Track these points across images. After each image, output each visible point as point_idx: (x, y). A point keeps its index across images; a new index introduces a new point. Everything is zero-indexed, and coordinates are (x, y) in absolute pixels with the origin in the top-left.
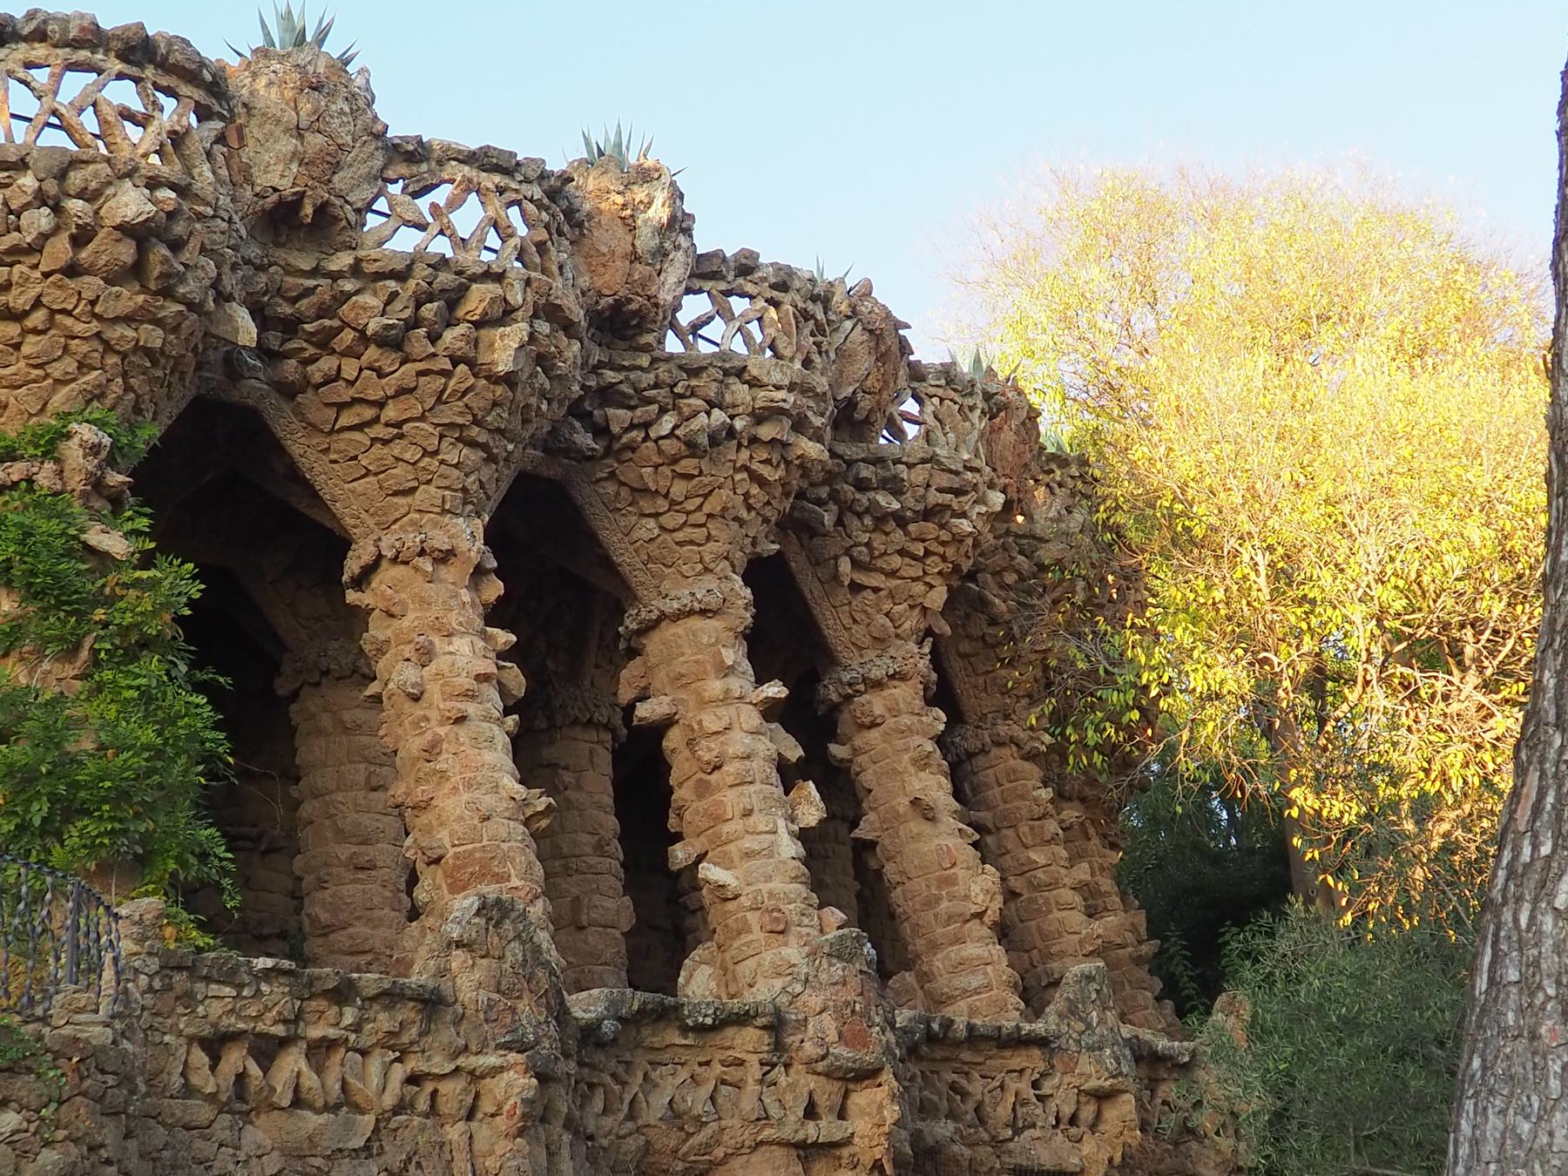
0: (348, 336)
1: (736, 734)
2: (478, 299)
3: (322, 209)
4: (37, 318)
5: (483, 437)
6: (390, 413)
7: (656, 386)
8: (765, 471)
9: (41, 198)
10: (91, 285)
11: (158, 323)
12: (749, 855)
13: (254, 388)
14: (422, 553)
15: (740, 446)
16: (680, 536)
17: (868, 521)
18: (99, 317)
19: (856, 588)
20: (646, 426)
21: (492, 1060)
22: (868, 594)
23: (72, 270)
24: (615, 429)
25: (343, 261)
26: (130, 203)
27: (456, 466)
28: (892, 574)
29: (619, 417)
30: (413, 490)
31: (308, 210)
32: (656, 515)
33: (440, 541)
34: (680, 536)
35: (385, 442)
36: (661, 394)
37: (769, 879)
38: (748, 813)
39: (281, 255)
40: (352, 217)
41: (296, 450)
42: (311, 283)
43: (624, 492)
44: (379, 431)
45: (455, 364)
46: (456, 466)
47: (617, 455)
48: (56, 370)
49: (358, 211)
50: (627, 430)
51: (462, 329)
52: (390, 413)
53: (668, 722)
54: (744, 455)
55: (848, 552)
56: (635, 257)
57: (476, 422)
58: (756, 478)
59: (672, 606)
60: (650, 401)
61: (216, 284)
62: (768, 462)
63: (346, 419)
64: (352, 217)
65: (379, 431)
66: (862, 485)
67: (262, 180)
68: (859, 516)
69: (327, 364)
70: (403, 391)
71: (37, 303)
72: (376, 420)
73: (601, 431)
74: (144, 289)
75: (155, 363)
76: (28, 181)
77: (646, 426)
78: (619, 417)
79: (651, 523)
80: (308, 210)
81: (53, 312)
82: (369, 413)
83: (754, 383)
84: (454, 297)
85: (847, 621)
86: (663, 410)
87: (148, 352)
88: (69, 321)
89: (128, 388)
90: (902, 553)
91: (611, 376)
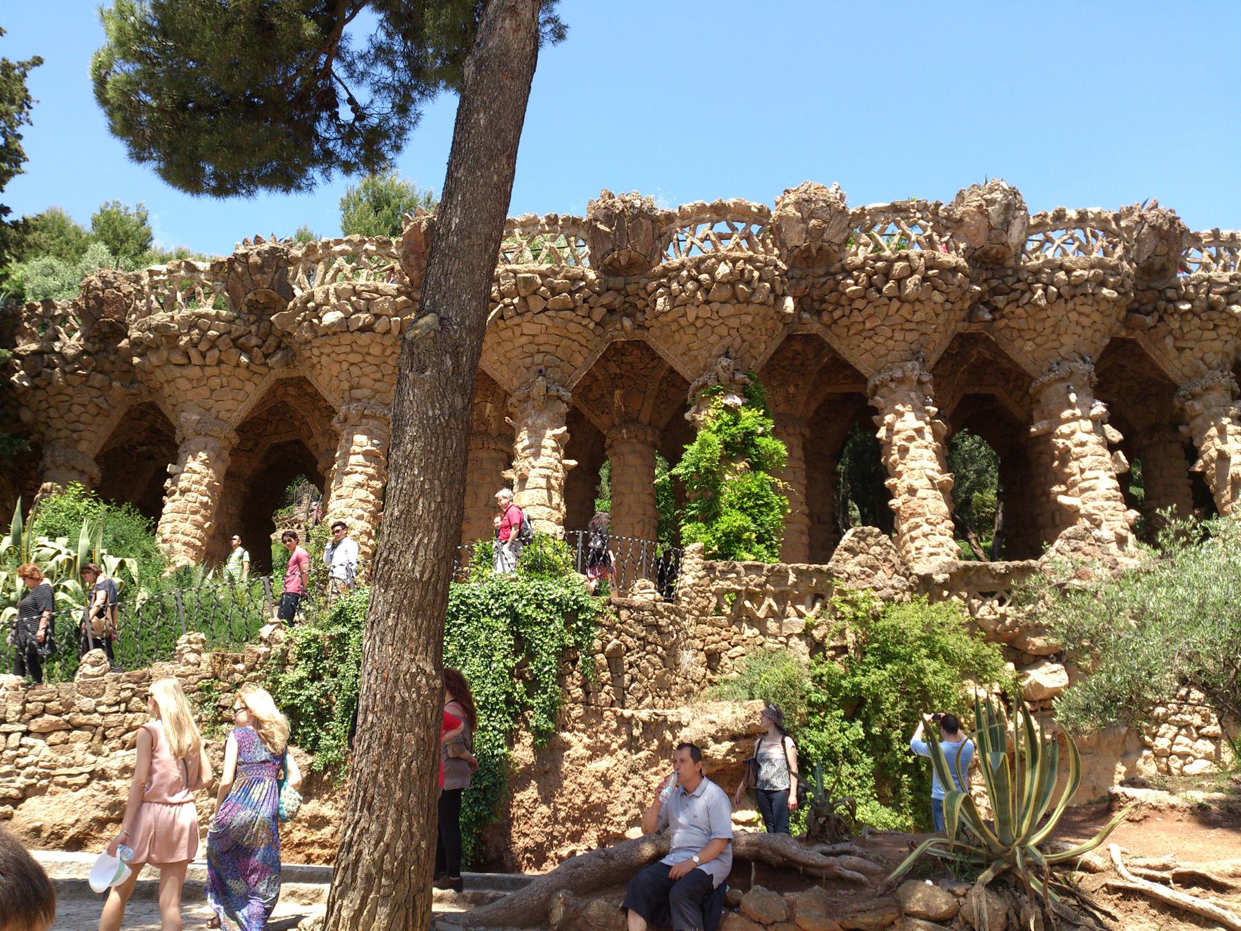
3: (820, 249)
4: (699, 323)
5: (913, 326)
6: (868, 325)
7: (1019, 281)
8: (1087, 309)
10: (716, 306)
13: (813, 326)
14: (892, 380)
15: (1066, 301)
16: (1047, 346)
19: (1180, 350)
20: (1017, 300)
23: (707, 302)
24: (1001, 305)
25: (838, 265)
26: (723, 269)
29: (1000, 301)
30: (886, 355)
31: (814, 252)
33: (898, 374)
34: (1047, 346)
35: (870, 338)
36: (1020, 286)
38: (1082, 471)
39: (811, 271)
40: (836, 248)
41: (836, 347)
42: (823, 280)
43: (1015, 333)
45: (890, 299)
47: (1003, 317)
49: (839, 245)
50: (1008, 304)
51: (891, 283)
52: (868, 325)
54: (1071, 305)
55: (1170, 333)
56: (991, 228)
58: (1080, 314)
60: (1015, 290)
61: (772, 290)
63: (852, 332)
64: (836, 248)
66: (1170, 301)
67: (790, 245)
68: (1172, 314)
69: (838, 313)
70: (870, 316)
71: (697, 318)
72: (863, 330)
73: (994, 310)
74: (739, 302)
76: (685, 273)
77: (1017, 300)
78: (1000, 301)
79: (1031, 343)
80: (814, 252)
82: (860, 327)
83: (1069, 272)
85: (1178, 366)
86: (1023, 292)
87: (748, 325)
88: (709, 322)
89: (743, 341)
91: (994, 283)
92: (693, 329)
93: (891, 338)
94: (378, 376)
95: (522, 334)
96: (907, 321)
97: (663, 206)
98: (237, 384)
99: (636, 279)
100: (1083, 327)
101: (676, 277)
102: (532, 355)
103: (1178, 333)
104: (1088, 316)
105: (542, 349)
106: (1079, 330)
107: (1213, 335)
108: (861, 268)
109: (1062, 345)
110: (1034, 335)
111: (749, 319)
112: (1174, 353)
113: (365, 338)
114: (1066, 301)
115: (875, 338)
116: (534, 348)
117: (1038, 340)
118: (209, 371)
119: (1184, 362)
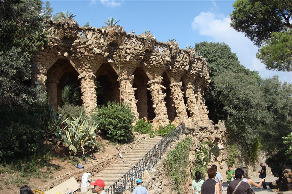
0: (175, 67)
1: (194, 99)
2: (185, 64)
9: (162, 58)
12: (195, 110)
18: (163, 68)
21: (197, 134)
28: (199, 82)
32: (188, 79)
37: (197, 112)
38: (195, 106)
41: (168, 75)
44: (175, 74)
48: (159, 72)
53: (188, 97)
59: (189, 87)
65: (175, 74)
76: (160, 57)
81: (160, 67)
84: (183, 64)
90: (201, 80)
92: (157, 69)
94: (95, 66)
95: (132, 64)
97: (159, 41)
98: (52, 58)
99: (147, 54)
101: (158, 57)
102: (130, 68)
105: (133, 67)
107: (201, 81)
108: (180, 62)
110: (189, 78)
113: (99, 56)
115: (176, 76)
116: (131, 67)
117: (189, 80)
118: (49, 54)
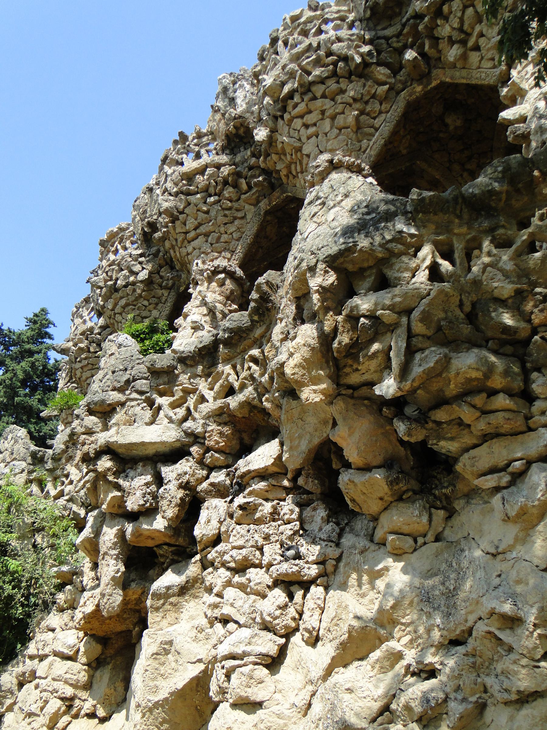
5: (192, 234)
8: (301, 108)
11: (121, 298)
17: (439, 22)
19: (477, 48)
22: (482, 42)
27: (194, 249)
32: (297, 173)
46: (194, 249)
54: (286, 116)
57: (186, 233)
62: (295, 106)
75: (135, 306)
79: (299, 175)
87: (127, 305)
93: (188, 254)
96: (186, 233)
100: (315, 124)
103: (456, 36)
104: (310, 112)
106: (312, 130)
109: (308, 156)
111: (123, 302)
112: (474, 57)
114: (282, 117)
119: (489, 55)
